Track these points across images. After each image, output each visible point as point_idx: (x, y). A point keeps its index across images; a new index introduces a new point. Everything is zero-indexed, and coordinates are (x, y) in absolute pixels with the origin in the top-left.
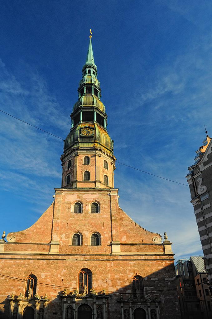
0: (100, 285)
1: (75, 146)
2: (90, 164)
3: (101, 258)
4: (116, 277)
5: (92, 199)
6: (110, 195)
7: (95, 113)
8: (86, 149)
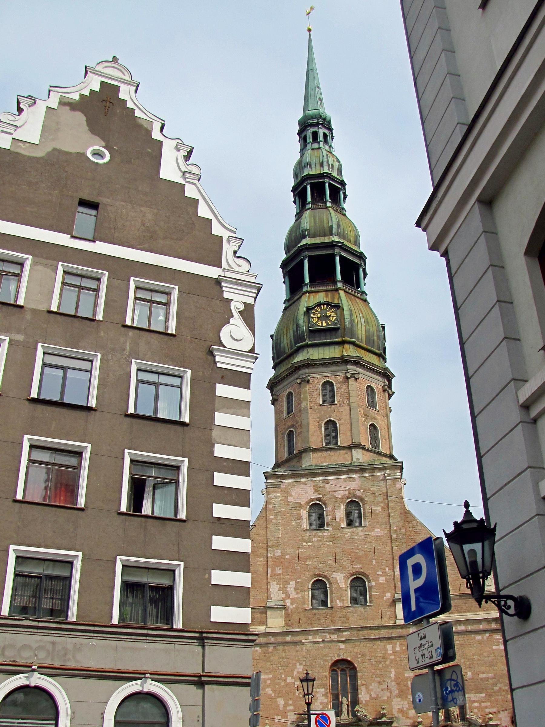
0: (374, 696)
1: (300, 358)
2: (336, 402)
3: (375, 634)
4: (406, 675)
7: (337, 259)
8: (325, 364)
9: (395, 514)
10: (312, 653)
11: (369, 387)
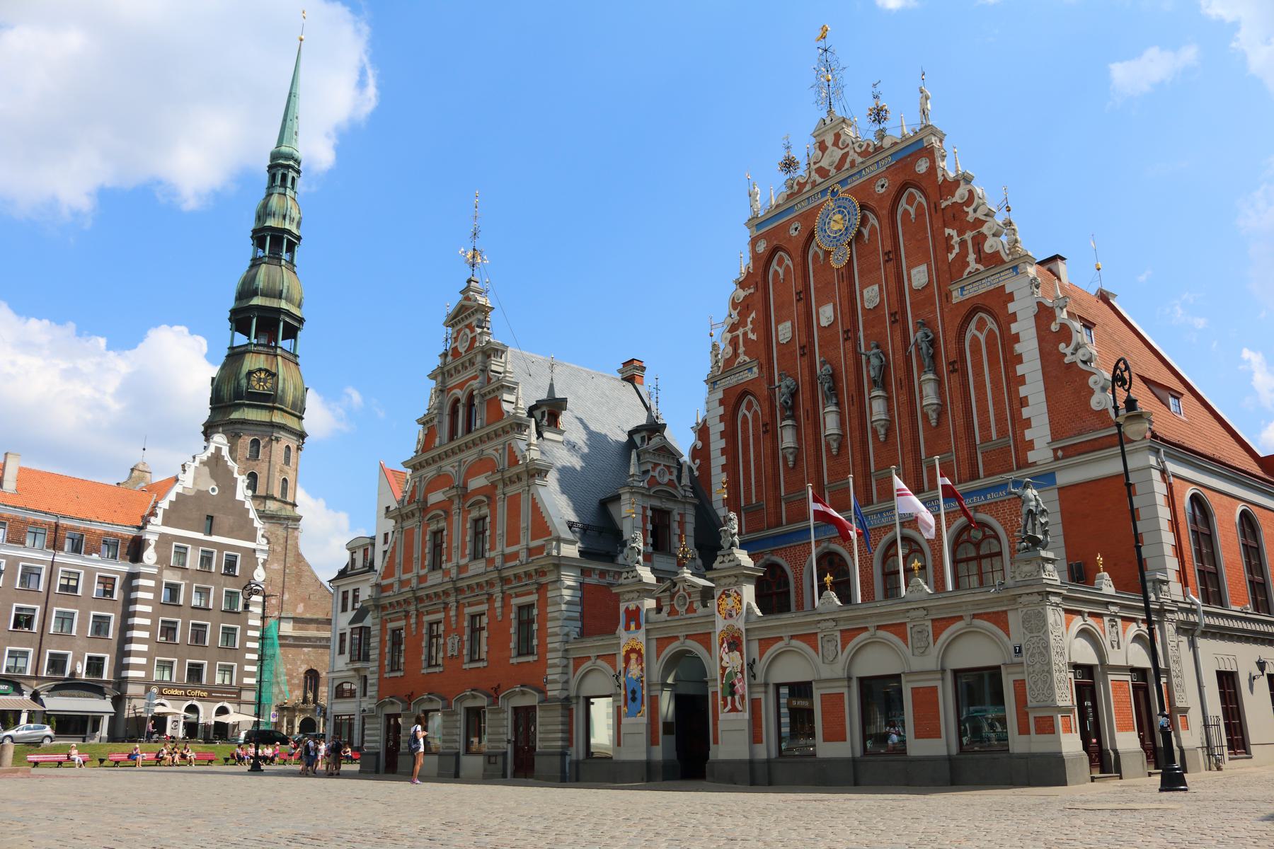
1: (235, 415)
9: (290, 554)
11: (288, 447)
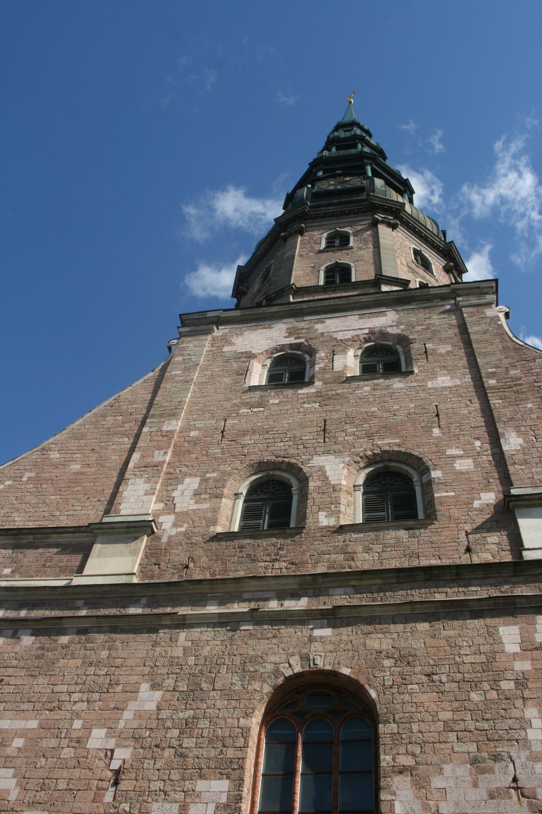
2: (351, 244)
5: (367, 331)
6: (457, 310)
10: (206, 651)
